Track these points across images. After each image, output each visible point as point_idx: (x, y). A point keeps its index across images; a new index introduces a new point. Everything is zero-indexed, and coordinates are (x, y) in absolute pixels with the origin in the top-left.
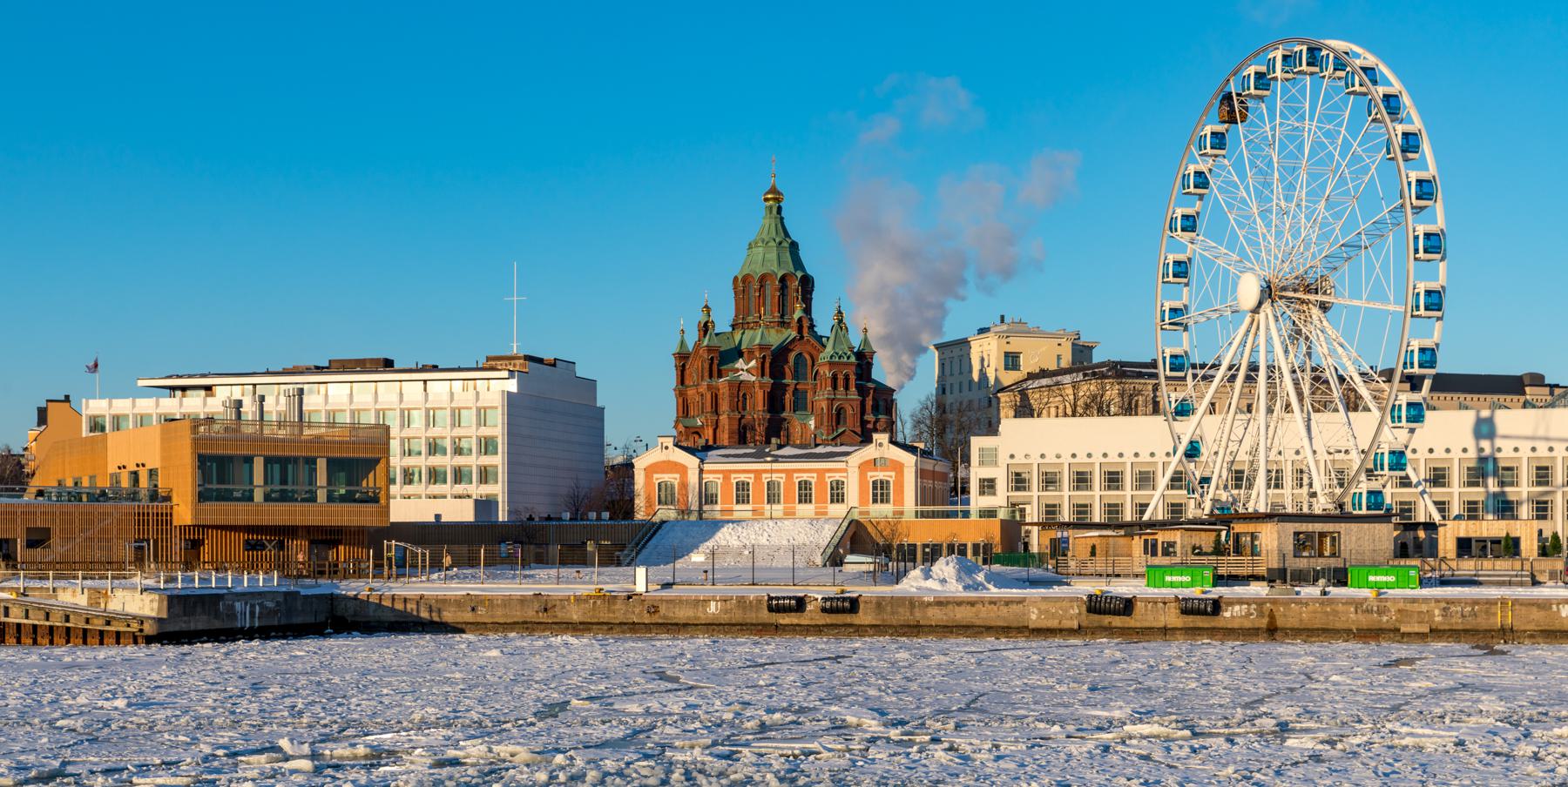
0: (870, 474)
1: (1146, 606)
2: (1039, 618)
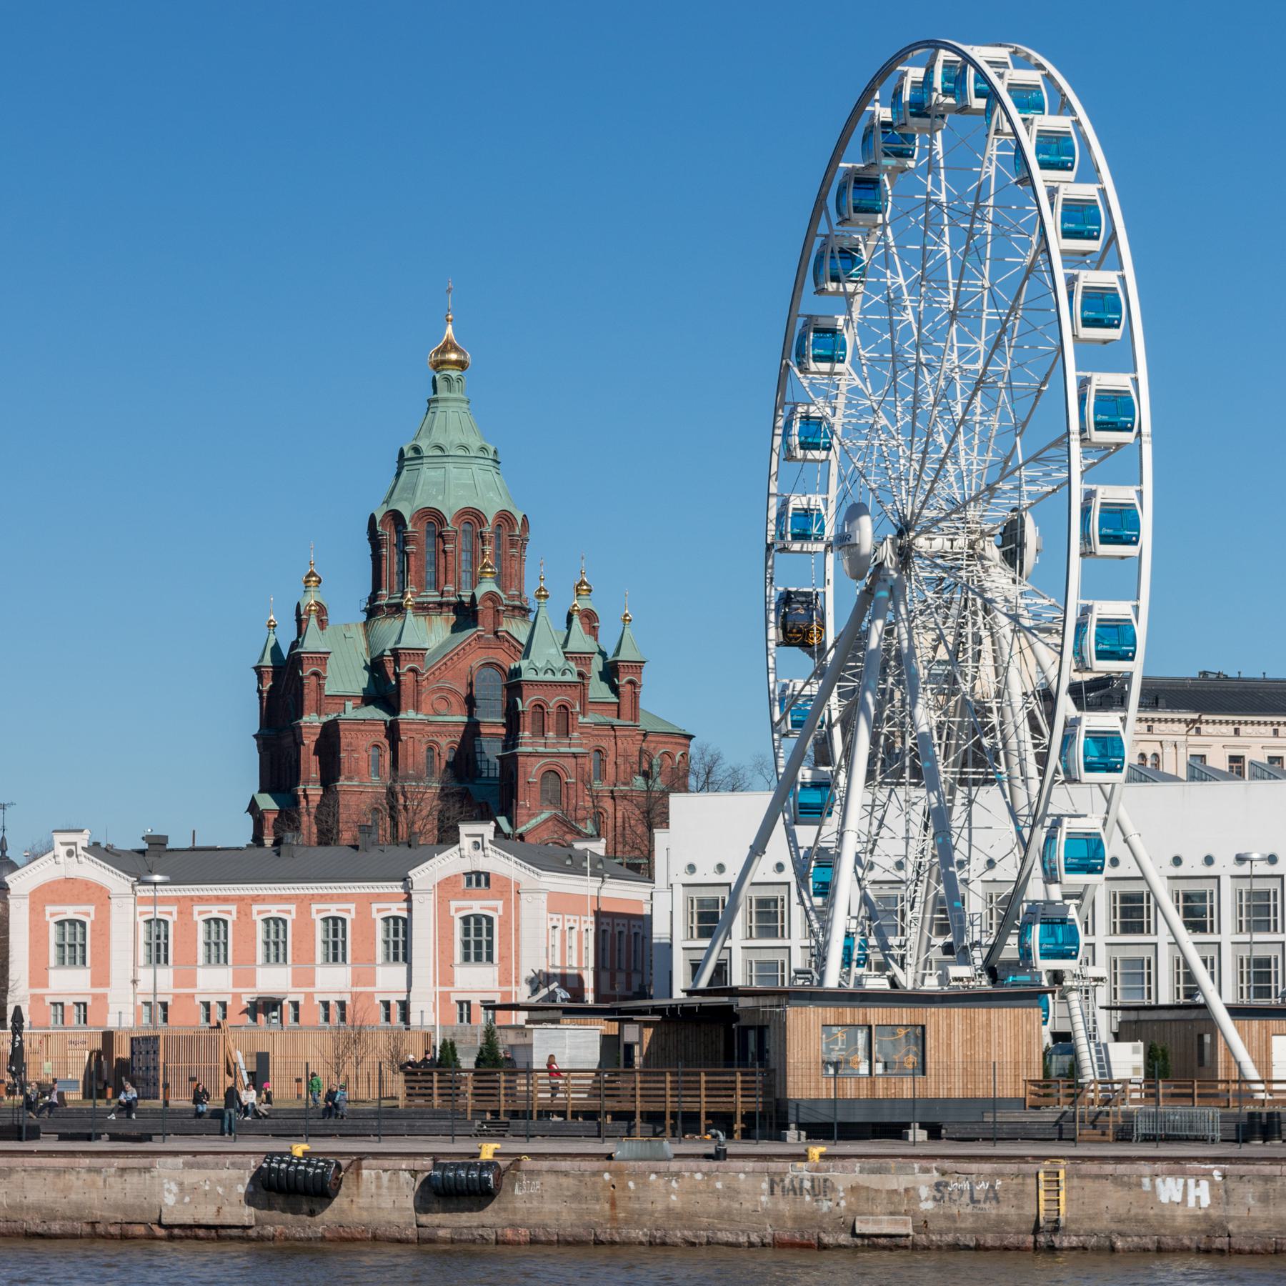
0: (454, 904)
1: (378, 1178)
2: (180, 1201)
